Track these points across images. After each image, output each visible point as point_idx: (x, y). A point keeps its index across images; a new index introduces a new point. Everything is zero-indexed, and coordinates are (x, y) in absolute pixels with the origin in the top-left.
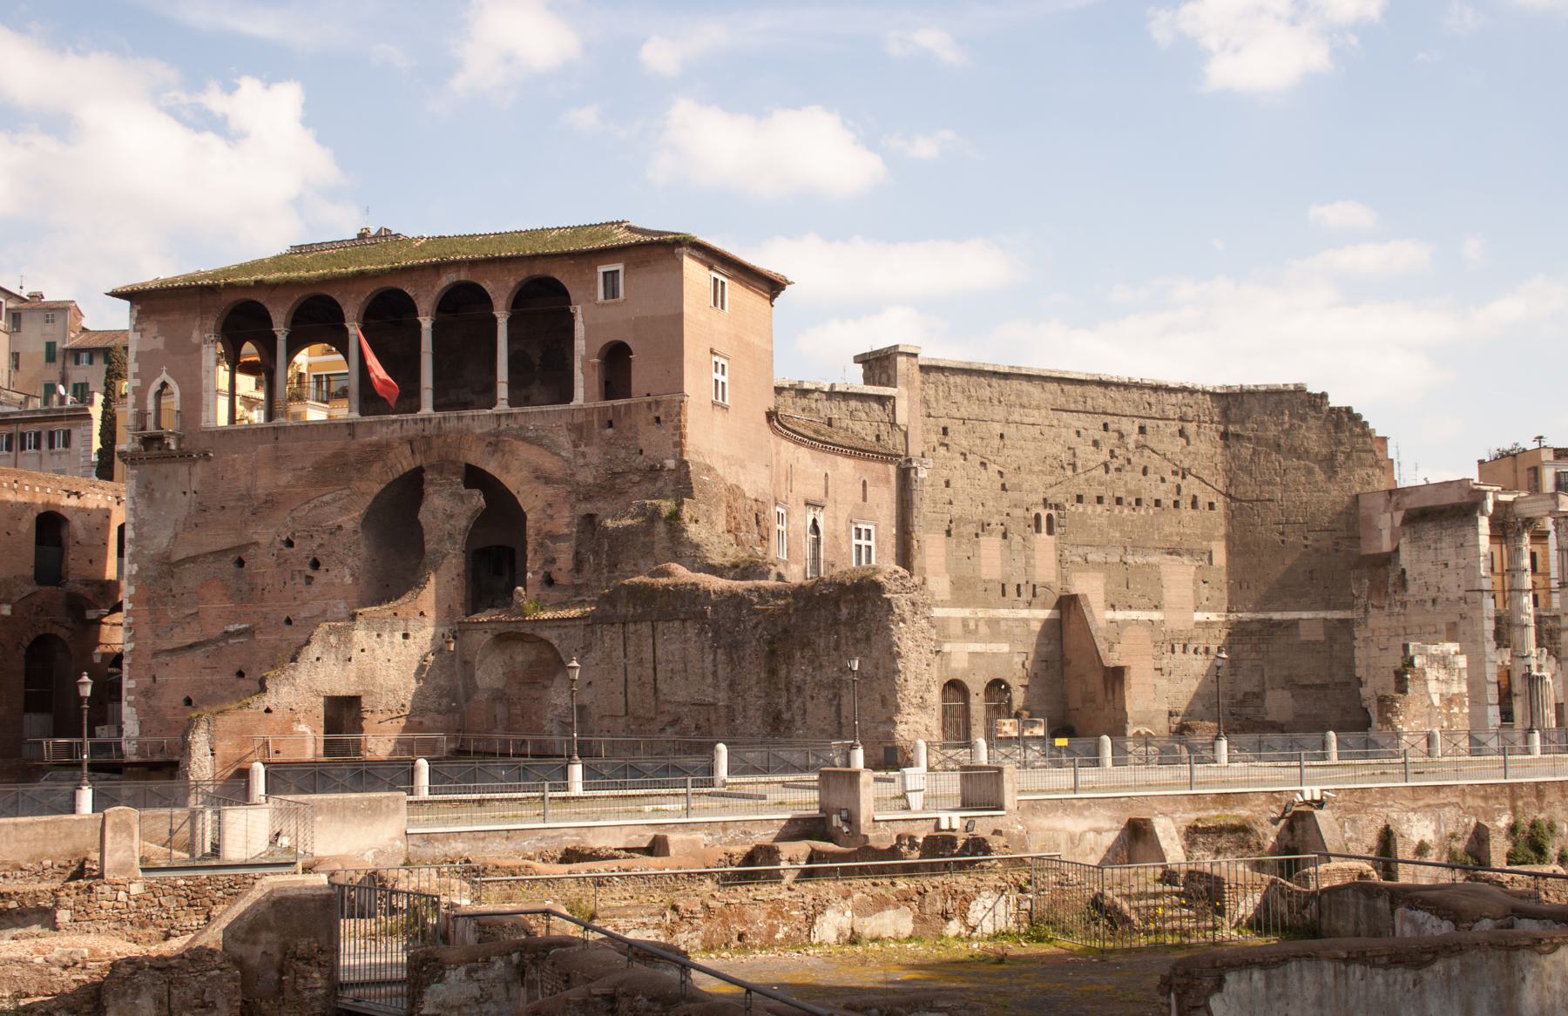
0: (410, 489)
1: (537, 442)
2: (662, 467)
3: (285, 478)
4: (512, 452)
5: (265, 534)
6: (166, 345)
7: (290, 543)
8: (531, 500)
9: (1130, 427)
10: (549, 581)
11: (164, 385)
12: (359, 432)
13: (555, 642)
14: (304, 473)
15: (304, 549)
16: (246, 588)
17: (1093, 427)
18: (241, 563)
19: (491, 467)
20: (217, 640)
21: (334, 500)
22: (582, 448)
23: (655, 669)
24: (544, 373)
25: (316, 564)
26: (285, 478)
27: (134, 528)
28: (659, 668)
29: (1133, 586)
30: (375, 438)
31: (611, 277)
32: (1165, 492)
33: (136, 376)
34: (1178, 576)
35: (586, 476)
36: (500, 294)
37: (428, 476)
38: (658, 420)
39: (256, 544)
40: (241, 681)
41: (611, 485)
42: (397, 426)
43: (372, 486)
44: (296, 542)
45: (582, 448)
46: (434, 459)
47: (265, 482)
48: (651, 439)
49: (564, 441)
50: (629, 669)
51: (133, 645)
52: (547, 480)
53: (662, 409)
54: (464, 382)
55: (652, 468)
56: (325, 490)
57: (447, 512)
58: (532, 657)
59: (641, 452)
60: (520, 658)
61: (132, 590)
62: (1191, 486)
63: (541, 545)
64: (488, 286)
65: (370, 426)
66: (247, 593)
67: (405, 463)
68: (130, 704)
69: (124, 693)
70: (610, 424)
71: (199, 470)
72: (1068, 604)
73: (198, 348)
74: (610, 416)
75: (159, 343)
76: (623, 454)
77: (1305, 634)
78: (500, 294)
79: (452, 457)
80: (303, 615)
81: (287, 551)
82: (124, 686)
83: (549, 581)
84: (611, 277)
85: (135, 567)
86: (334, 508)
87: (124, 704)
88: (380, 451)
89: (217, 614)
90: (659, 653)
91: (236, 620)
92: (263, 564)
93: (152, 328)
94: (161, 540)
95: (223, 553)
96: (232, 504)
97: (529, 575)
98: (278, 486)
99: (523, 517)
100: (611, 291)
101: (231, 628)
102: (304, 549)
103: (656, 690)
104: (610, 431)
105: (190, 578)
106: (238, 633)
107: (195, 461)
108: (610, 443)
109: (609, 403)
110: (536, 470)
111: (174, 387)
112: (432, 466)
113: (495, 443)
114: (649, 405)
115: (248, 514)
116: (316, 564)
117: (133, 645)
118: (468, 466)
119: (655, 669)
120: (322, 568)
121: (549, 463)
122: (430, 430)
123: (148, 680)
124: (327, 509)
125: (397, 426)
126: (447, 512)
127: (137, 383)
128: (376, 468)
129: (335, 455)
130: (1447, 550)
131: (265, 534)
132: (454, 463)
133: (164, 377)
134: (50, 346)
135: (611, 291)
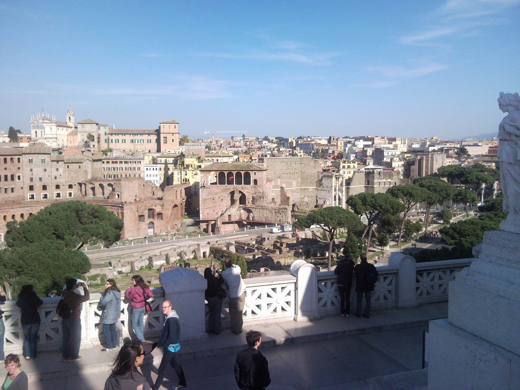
5: (216, 197)
9: (289, 164)
15: (221, 198)
17: (285, 164)
24: (248, 182)
29: (290, 184)
31: (255, 173)
32: (293, 172)
34: (294, 183)
35: (252, 192)
36: (243, 173)
41: (255, 193)
47: (216, 191)
49: (250, 189)
54: (239, 182)
57: (237, 196)
62: (296, 171)
64: (241, 172)
72: (282, 188)
77: (310, 190)
78: (243, 173)
84: (255, 173)
88: (229, 189)
89: (211, 205)
92: (216, 199)
93: (202, 174)
94: (204, 197)
100: (255, 174)
105: (208, 201)
113: (242, 188)
121: (249, 191)
126: (237, 196)
130: (329, 180)
131: (216, 197)
134: (105, 133)
135: (255, 174)
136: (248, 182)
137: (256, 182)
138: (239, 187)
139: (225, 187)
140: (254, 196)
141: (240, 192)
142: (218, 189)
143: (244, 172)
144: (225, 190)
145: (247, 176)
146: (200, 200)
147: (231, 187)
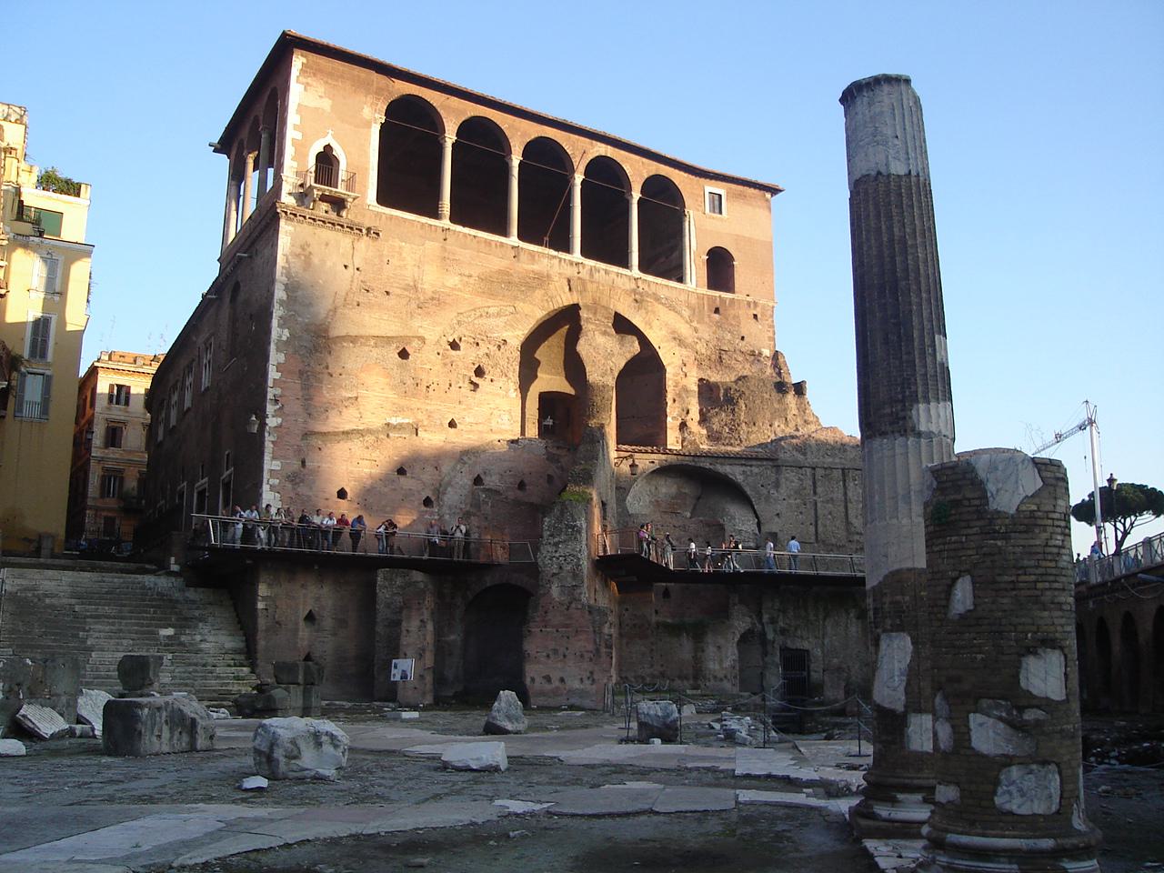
0: (566, 321)
1: (672, 308)
2: (760, 354)
3: (453, 280)
4: (654, 312)
6: (332, 106)
7: (454, 346)
8: (670, 357)
10: (683, 426)
11: (328, 148)
12: (523, 257)
13: (740, 478)
14: (472, 281)
15: (468, 356)
16: (410, 382)
18: (404, 354)
19: (637, 321)
20: (378, 431)
21: (498, 315)
22: (695, 324)
23: (846, 508)
24: (663, 257)
25: (479, 372)
26: (453, 280)
27: (286, 285)
28: (849, 505)
30: (536, 267)
33: (296, 127)
37: (584, 314)
38: (755, 316)
39: (422, 339)
40: (402, 479)
42: (556, 261)
43: (535, 312)
44: (462, 345)
45: (695, 324)
46: (589, 302)
47: (431, 278)
48: (749, 328)
49: (686, 313)
50: (819, 505)
51: (280, 420)
52: (681, 342)
53: (758, 309)
55: (753, 354)
56: (491, 302)
58: (673, 490)
59: (743, 338)
60: (664, 490)
61: (281, 358)
63: (679, 395)
65: (532, 254)
66: (415, 388)
67: (566, 299)
68: (272, 488)
69: (266, 475)
70: (717, 311)
71: (364, 243)
73: (368, 125)
74: (718, 304)
75: (326, 104)
76: (729, 336)
79: (604, 303)
80: (467, 420)
81: (453, 352)
82: (266, 467)
83: (683, 426)
85: (286, 332)
86: (500, 321)
87: (265, 487)
88: (541, 280)
90: (850, 494)
91: (400, 410)
92: (427, 360)
93: (319, 87)
95: (388, 340)
96: (399, 291)
97: (669, 419)
98: (444, 286)
99: (660, 368)
101: (394, 421)
102: (468, 356)
103: (848, 523)
104: (717, 316)
106: (400, 427)
107: (360, 236)
108: (719, 325)
109: (717, 293)
110: (673, 332)
111: (338, 152)
112: (587, 307)
114: (749, 303)
115: (414, 306)
116: (479, 372)
117: (280, 420)
118: (616, 313)
119: (846, 508)
120: (488, 377)
121: (685, 330)
122: (584, 274)
123: (296, 464)
124: (492, 321)
125: (556, 261)
127: (298, 136)
128: (539, 293)
129: (500, 272)
131: (433, 330)
132: (606, 308)
133: (329, 140)
136: (663, 257)
137: (720, 267)
138: (619, 285)
139: (496, 263)
140: (714, 377)
141: (622, 326)
142: (446, 261)
143: (647, 168)
144: (501, 285)
145: (664, 205)
146: (277, 332)
147: (565, 273)
